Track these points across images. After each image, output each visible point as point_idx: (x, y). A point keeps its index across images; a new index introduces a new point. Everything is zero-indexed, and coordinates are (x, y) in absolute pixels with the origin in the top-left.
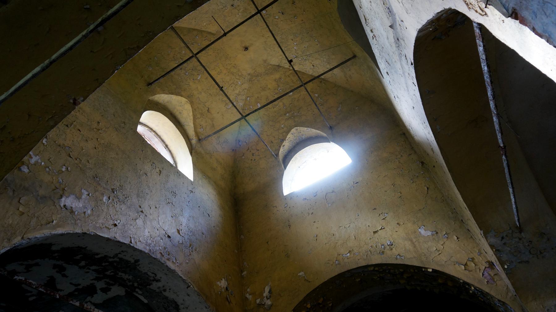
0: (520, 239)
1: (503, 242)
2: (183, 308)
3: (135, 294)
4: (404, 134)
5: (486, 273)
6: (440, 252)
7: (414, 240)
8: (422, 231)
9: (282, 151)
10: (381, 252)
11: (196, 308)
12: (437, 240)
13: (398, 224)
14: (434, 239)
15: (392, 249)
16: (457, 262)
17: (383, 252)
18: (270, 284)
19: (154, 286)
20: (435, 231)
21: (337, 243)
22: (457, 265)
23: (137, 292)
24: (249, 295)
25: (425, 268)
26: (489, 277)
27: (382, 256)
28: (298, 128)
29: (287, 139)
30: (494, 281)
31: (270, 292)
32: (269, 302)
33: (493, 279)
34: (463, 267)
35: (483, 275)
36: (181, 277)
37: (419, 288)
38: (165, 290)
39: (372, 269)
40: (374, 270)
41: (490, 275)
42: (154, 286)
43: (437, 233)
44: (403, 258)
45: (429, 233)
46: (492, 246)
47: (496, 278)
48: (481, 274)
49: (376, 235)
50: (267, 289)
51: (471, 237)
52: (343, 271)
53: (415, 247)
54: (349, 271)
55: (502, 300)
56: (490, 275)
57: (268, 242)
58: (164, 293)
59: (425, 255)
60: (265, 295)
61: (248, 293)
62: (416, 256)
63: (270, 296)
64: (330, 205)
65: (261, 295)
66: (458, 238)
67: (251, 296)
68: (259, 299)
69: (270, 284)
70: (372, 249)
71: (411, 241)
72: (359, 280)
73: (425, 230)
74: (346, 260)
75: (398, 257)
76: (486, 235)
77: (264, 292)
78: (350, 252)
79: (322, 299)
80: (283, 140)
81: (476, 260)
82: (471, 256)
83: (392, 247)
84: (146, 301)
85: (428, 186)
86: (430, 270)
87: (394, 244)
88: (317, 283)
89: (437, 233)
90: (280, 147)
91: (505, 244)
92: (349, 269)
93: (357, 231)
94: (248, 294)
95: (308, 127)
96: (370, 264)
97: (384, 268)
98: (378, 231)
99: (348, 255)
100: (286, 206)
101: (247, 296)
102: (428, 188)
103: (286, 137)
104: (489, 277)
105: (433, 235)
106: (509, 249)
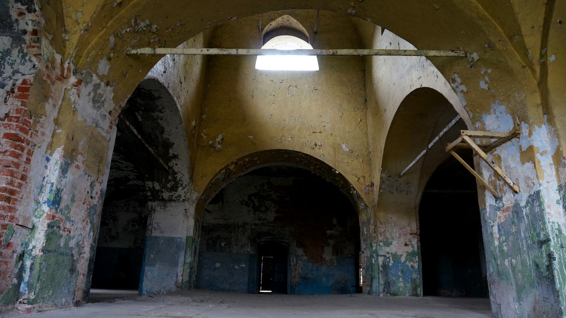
0: (397, 181)
1: (388, 178)
2: (167, 134)
3: (137, 114)
4: (364, 71)
5: (367, 188)
6: (348, 165)
7: (337, 150)
8: (344, 146)
9: (267, 28)
10: (313, 147)
11: (176, 138)
12: (350, 156)
13: (331, 134)
14: (348, 155)
15: (320, 149)
16: (355, 175)
17: (314, 148)
18: (223, 134)
19: (156, 114)
20: (352, 150)
21: (285, 127)
22: (354, 177)
23: (139, 113)
24: (205, 135)
25: (335, 169)
26: (367, 191)
27: (312, 150)
28: (290, 16)
29: (276, 20)
30: (369, 194)
31: (222, 139)
32: (219, 146)
33: (369, 192)
34: (357, 179)
35: (365, 188)
36: (181, 116)
37: (318, 175)
38: (161, 119)
39: (301, 155)
40: (302, 156)
41: (369, 190)
42: (156, 114)
43: (352, 152)
44: (325, 158)
45: (348, 150)
46: (381, 178)
47: (371, 192)
48: (364, 187)
49: (314, 134)
50: (220, 137)
51: (370, 164)
52: (282, 148)
53: (335, 154)
54: (286, 150)
55: (368, 205)
56: (369, 190)
57: (230, 101)
58: (159, 121)
59: (339, 162)
60: (217, 140)
61: (203, 132)
62: (333, 160)
63: (221, 143)
64: (290, 96)
65: (214, 139)
66: (362, 161)
67: (205, 136)
68: (212, 142)
69: (223, 134)
70: (307, 143)
71: (334, 149)
72: (287, 156)
73: (346, 147)
74: (287, 142)
75: (322, 156)
76: (383, 171)
77: (218, 138)
78: (291, 138)
79: (257, 158)
80: (272, 20)
81: (366, 178)
82: (364, 175)
83: (321, 147)
84: (140, 120)
85: (362, 119)
86: (338, 172)
87: (323, 146)
88: (261, 149)
89: (352, 152)
90: (268, 24)
91: (388, 180)
92: (287, 149)
93: (302, 125)
94: (203, 134)
95: (298, 21)
96: (302, 152)
97: (308, 157)
98: (316, 132)
99: (290, 139)
100: (254, 78)
101: (203, 135)
102: (361, 120)
103: (276, 19)
104: (367, 191)
105: (349, 152)
106: (388, 183)
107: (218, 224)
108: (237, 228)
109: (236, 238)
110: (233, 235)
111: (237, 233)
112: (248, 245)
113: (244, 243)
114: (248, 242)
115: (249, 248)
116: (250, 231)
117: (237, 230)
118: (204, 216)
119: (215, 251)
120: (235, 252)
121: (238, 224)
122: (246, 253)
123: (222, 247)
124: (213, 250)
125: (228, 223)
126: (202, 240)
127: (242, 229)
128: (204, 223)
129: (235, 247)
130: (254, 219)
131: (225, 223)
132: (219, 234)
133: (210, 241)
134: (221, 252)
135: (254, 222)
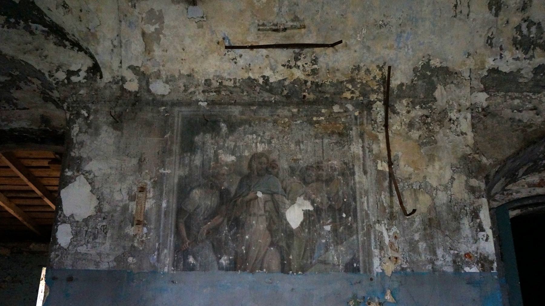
107: (251, 83)
108: (379, 108)
109: (383, 166)
110: (356, 148)
111: (381, 136)
112: (475, 215)
113: (442, 198)
114: (472, 190)
115: (490, 232)
116: (465, 125)
117: (380, 118)
118: (151, 29)
119: (234, 266)
120: (390, 268)
121: (386, 81)
122: (474, 269)
123: (290, 233)
124: (224, 261)
125: (314, 72)
126: (142, 189)
127: (418, 112)
128: (158, 76)
129: (382, 228)
130: (490, 42)
131: (298, 74)
132: (261, 148)
133: (196, 194)
134: (285, 268)
135: (490, 63)
